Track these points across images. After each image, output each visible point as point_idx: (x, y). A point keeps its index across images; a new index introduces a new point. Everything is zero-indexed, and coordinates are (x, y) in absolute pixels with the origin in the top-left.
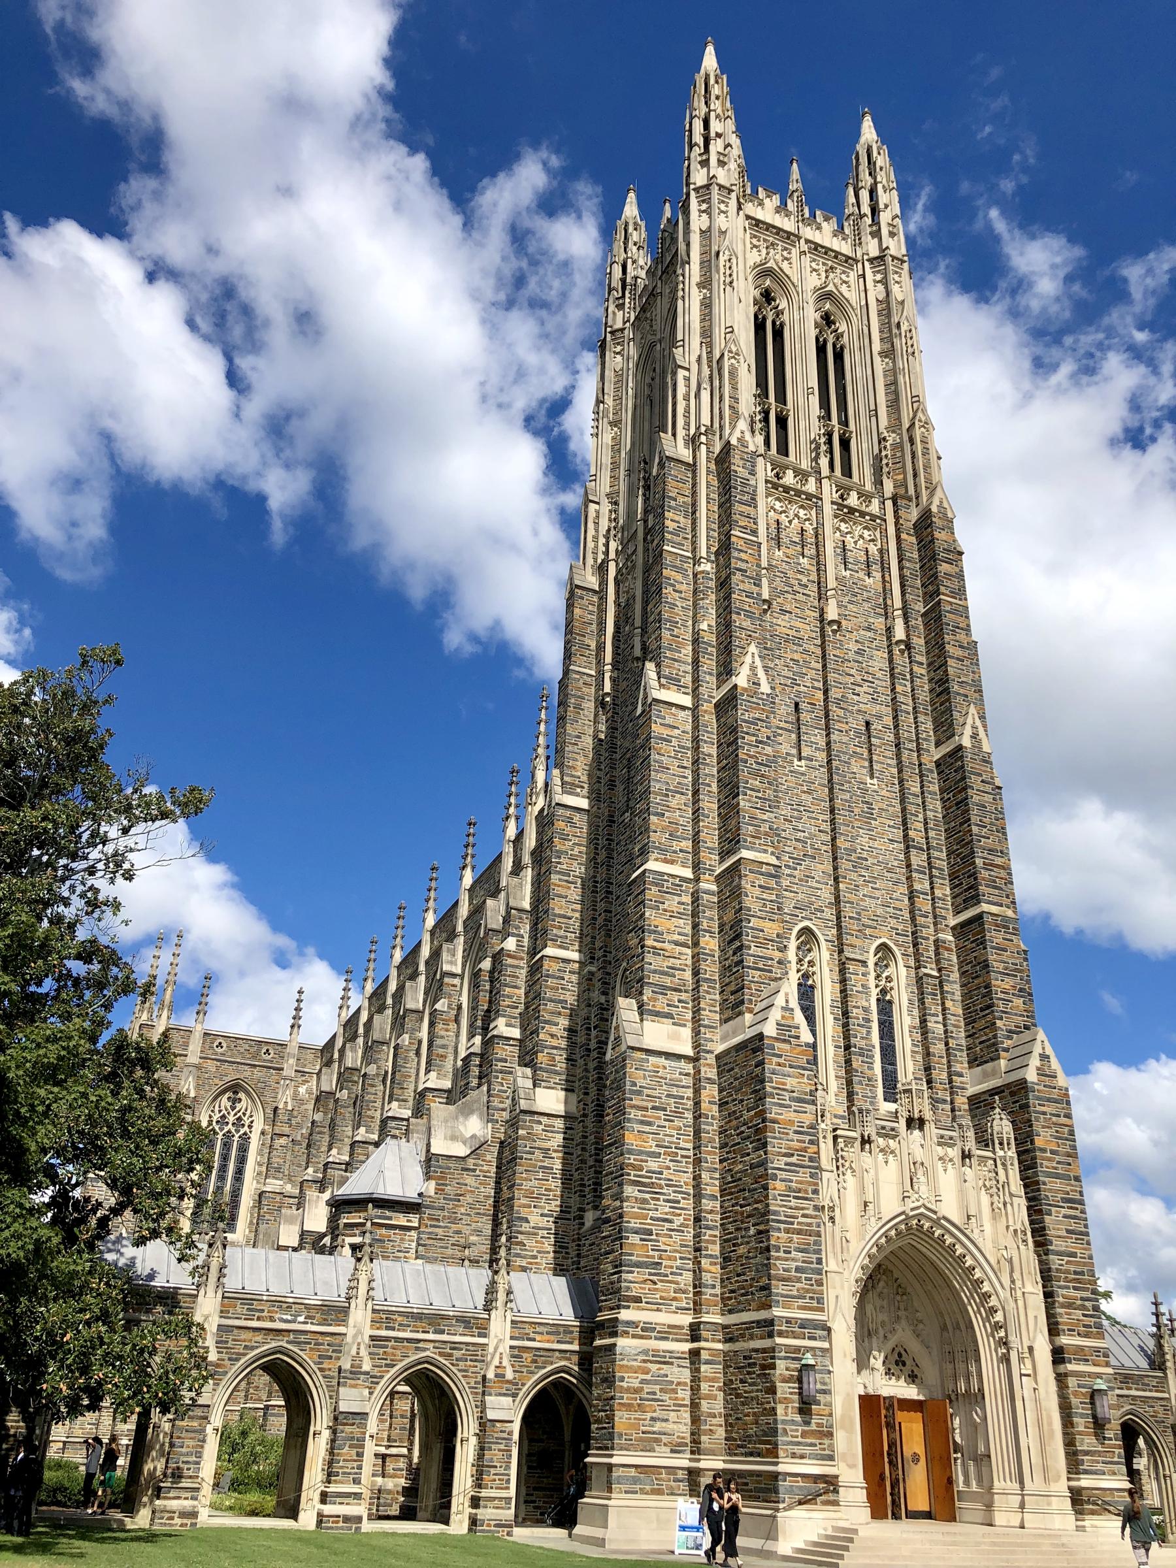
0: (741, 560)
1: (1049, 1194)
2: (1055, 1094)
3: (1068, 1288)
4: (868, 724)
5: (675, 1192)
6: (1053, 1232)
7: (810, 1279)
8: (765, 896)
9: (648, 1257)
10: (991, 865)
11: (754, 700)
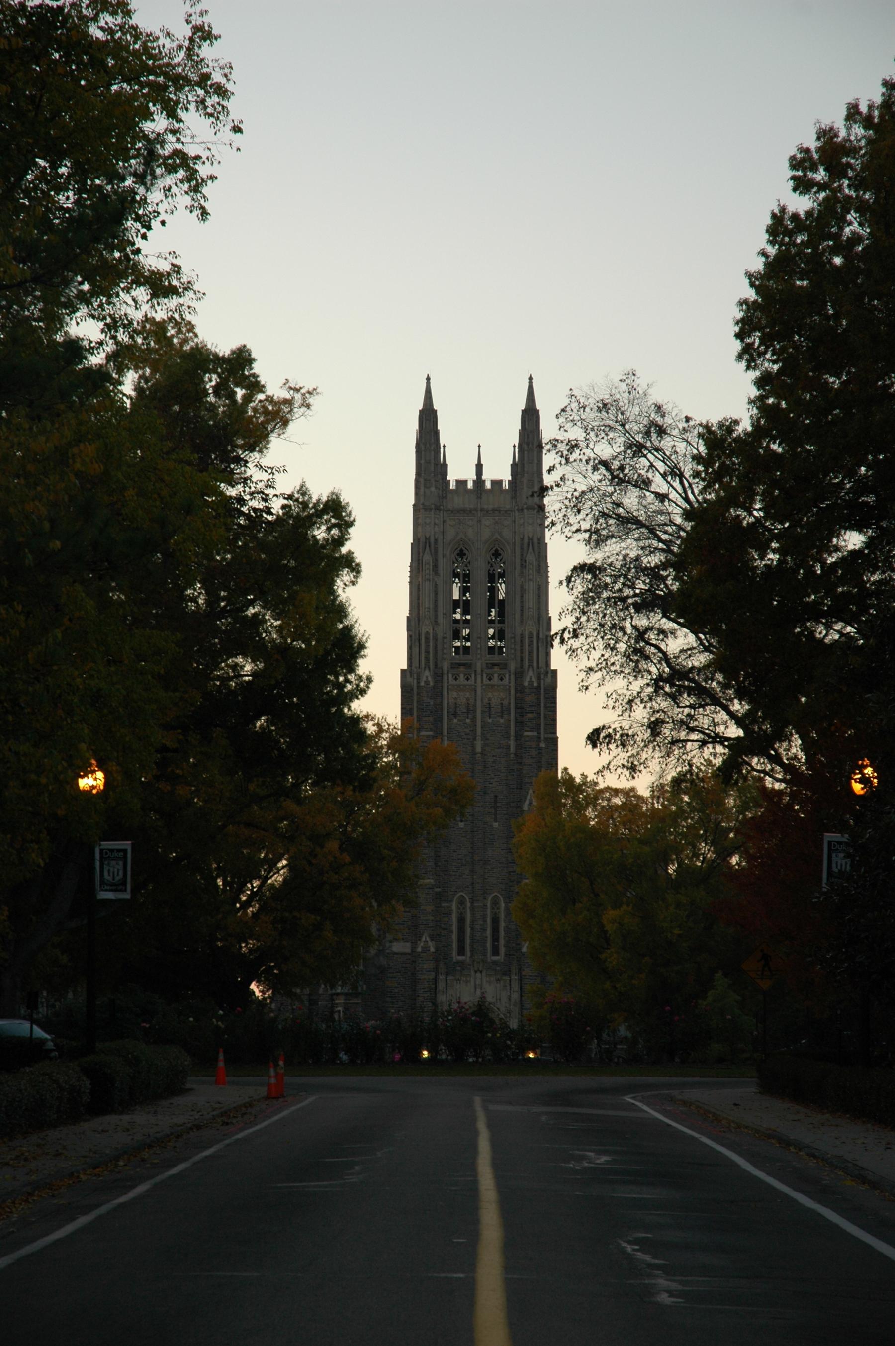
4: (496, 796)
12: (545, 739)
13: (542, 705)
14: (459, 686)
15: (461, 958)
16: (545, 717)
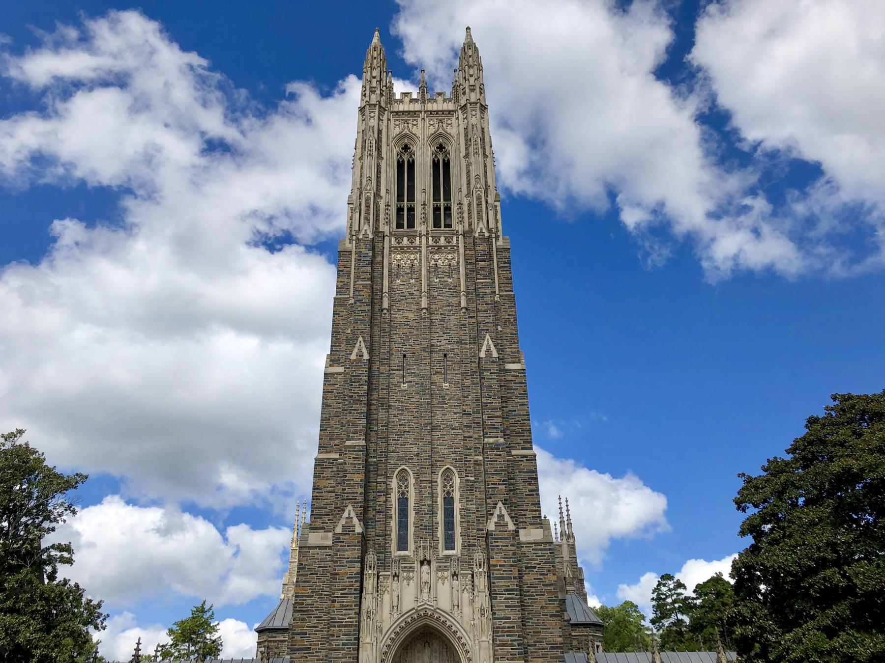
0: (360, 295)
1: (496, 588)
2: (506, 535)
3: (504, 636)
4: (445, 356)
5: (319, 613)
6: (497, 608)
7: (350, 648)
8: (355, 462)
9: (304, 645)
10: (492, 417)
11: (360, 364)
12: (501, 296)
13: (495, 261)
14: (402, 248)
15: (403, 553)
16: (499, 276)
